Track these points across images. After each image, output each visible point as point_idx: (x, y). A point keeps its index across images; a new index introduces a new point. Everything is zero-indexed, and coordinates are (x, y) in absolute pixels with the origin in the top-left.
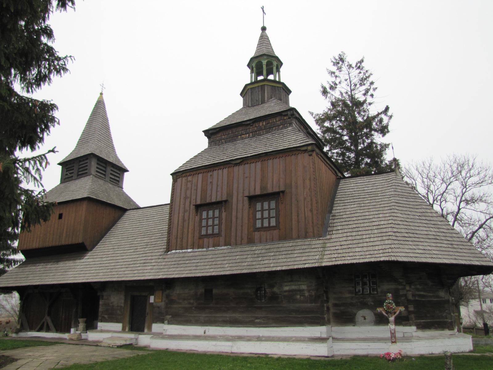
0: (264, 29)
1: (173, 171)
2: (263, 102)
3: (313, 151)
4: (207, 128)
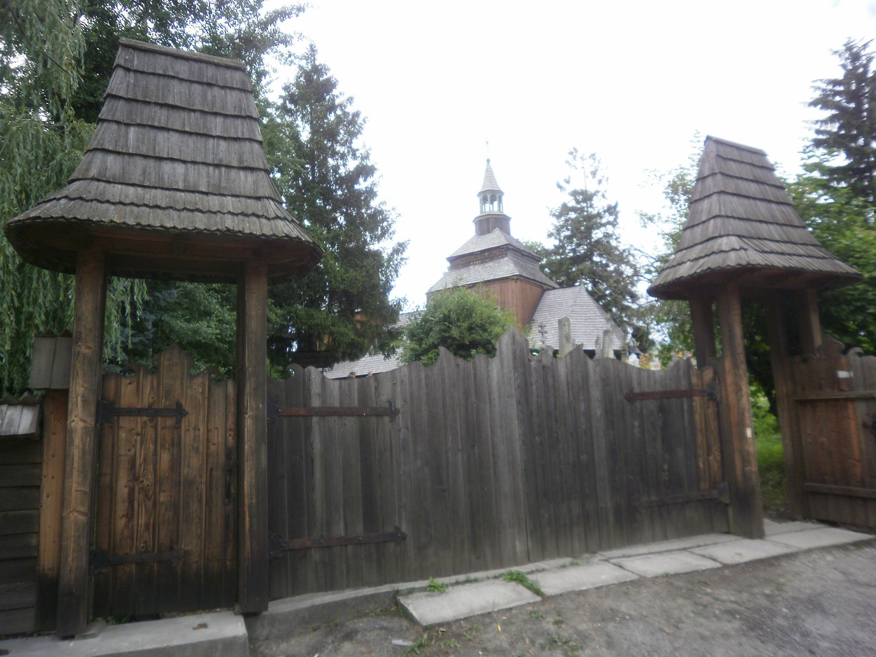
0: (488, 161)
1: (426, 292)
2: (489, 232)
3: (517, 279)
4: (448, 256)
